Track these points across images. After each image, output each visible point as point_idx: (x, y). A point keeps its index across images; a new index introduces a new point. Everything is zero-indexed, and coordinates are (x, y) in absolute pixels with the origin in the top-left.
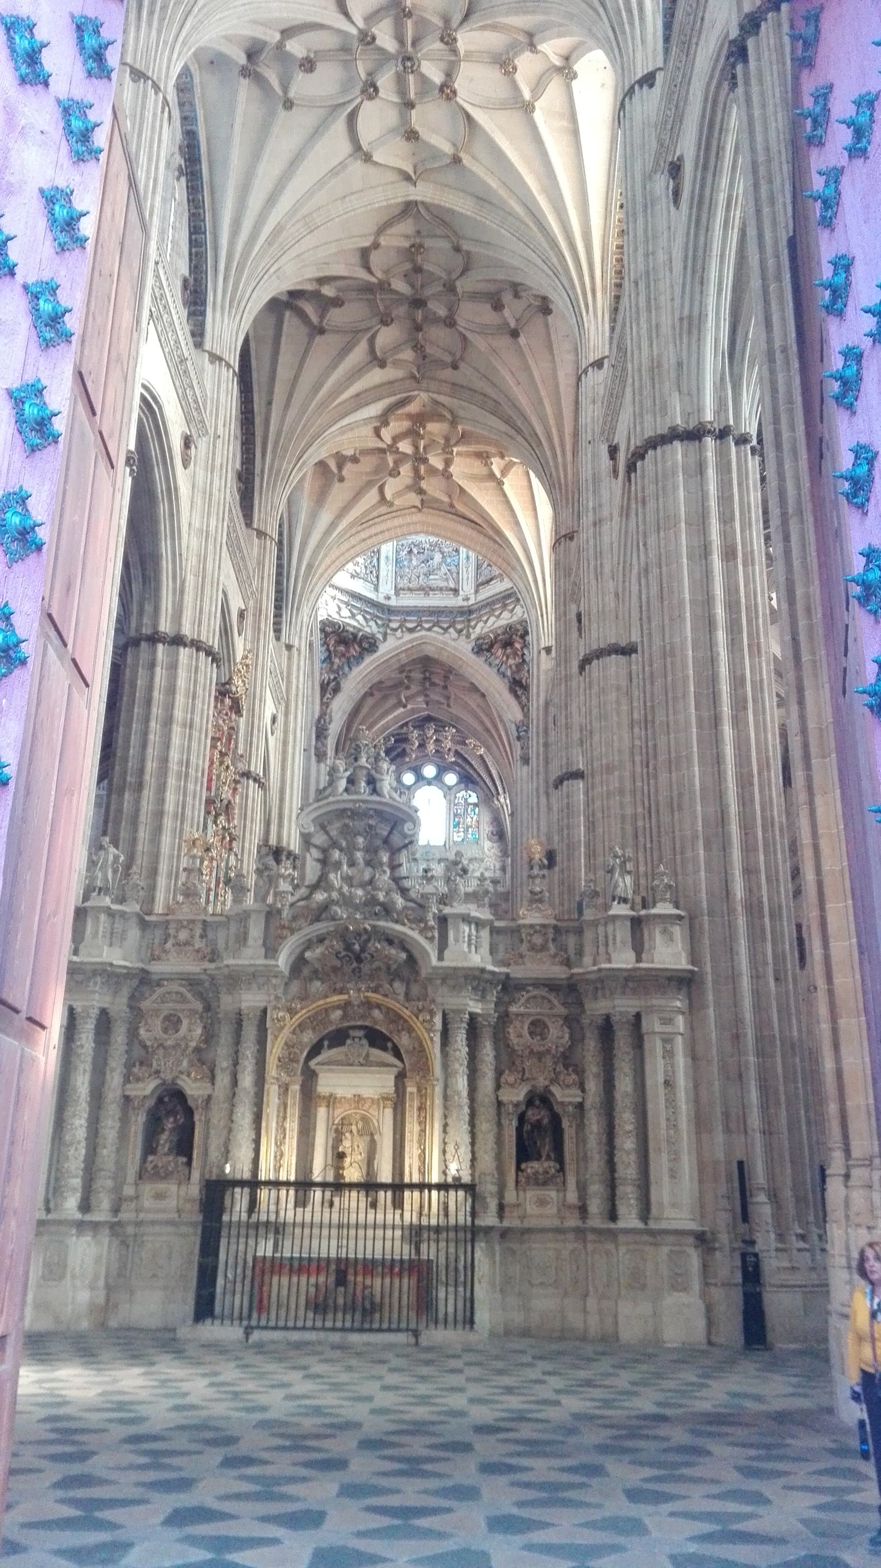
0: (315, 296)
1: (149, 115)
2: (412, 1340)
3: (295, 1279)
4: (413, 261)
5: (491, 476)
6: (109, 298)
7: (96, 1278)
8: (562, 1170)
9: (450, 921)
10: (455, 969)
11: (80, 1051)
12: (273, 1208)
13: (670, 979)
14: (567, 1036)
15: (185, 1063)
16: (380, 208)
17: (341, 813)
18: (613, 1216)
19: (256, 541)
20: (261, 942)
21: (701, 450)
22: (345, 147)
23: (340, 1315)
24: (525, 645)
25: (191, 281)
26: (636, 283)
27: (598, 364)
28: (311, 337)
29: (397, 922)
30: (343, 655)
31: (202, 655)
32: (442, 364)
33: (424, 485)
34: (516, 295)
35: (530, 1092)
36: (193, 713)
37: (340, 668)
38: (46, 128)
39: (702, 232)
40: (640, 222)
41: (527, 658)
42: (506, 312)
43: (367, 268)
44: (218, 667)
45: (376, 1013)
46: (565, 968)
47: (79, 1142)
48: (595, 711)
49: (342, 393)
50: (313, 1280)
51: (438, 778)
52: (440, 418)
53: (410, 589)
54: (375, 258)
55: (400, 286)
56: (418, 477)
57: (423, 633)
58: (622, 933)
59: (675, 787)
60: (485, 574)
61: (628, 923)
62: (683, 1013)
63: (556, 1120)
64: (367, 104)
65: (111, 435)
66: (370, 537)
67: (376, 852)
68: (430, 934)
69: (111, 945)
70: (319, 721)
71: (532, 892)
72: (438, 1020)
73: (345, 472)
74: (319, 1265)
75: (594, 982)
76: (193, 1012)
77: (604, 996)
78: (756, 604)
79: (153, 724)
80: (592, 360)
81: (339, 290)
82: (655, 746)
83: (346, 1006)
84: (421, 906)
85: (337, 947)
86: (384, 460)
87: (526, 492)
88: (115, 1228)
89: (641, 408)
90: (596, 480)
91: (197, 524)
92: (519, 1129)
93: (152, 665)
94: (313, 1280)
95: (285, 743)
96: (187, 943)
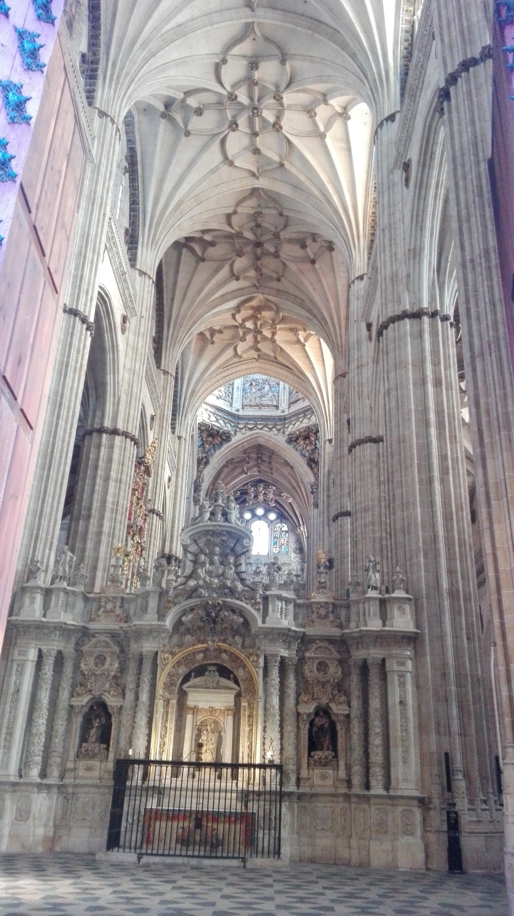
0: (200, 240)
1: (108, 137)
2: (242, 864)
3: (170, 824)
4: (256, 221)
5: (299, 342)
6: (58, 186)
7: (48, 819)
8: (336, 756)
9: (270, 599)
10: (273, 629)
11: (44, 677)
12: (157, 777)
13: (403, 637)
14: (340, 672)
15: (107, 685)
16: (237, 192)
17: (207, 533)
18: (367, 786)
19: (162, 376)
20: (156, 610)
21: (421, 324)
22: (219, 158)
23: (197, 847)
24: (317, 439)
25: (130, 230)
26: (383, 230)
27: (361, 278)
28: (197, 263)
29: (238, 599)
30: (211, 443)
31: (128, 440)
32: (271, 278)
33: (259, 346)
34: (314, 240)
36: (121, 474)
37: (209, 450)
38: (5, 43)
39: (422, 202)
40: (386, 196)
41: (318, 446)
42: (308, 250)
43: (230, 224)
44: (138, 447)
45: (224, 656)
47: (41, 734)
48: (358, 476)
49: (214, 293)
50: (181, 825)
51: (265, 516)
52: (270, 309)
53: (250, 406)
54: (235, 220)
55: (248, 235)
56: (256, 342)
57: (258, 431)
58: (374, 608)
59: (406, 520)
60: (294, 398)
61: (378, 603)
62: (411, 659)
63: (333, 724)
64: (232, 134)
65: (56, 271)
67: (226, 556)
68: (257, 607)
69: (66, 612)
70: (196, 481)
71: (319, 582)
72: (261, 661)
73: (215, 339)
74: (185, 815)
75: (356, 639)
76: (113, 653)
77: (363, 647)
78: (454, 413)
79: (98, 480)
80: (357, 276)
81: (214, 237)
82: (394, 495)
83: (206, 651)
84: (253, 590)
86: (238, 333)
87: (318, 350)
88: (61, 788)
89: (386, 299)
90: (359, 342)
91: (128, 366)
92: (310, 731)
93: (99, 446)
94: (181, 825)
95: (176, 493)
96: (112, 611)
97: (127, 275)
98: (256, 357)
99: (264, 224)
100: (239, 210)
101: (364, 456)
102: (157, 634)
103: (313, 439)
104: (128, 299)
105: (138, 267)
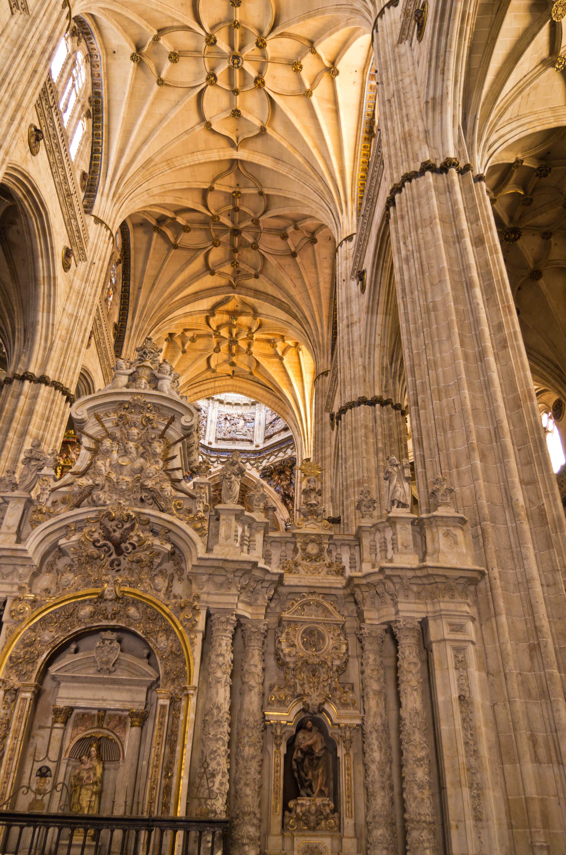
5: (276, 355)
9: (222, 517)
14: (344, 647)
22: (195, 118)
25: (89, 177)
26: (389, 101)
28: (169, 250)
31: (59, 393)
32: (248, 276)
33: (234, 359)
34: (296, 228)
35: (303, 710)
36: (44, 431)
42: (289, 241)
43: (206, 207)
45: (132, 611)
46: (340, 578)
52: (247, 314)
53: (224, 440)
54: (211, 199)
60: (271, 431)
62: (473, 619)
66: (200, 392)
67: (150, 444)
68: (199, 525)
72: (201, 619)
79: (11, 434)
80: (345, 236)
81: (188, 221)
85: (96, 536)
90: (348, 301)
97: (74, 197)
98: (231, 374)
99: (243, 208)
100: (216, 187)
101: (356, 421)
102: (11, 568)
103: (288, 473)
104: (76, 233)
105: (94, 212)
